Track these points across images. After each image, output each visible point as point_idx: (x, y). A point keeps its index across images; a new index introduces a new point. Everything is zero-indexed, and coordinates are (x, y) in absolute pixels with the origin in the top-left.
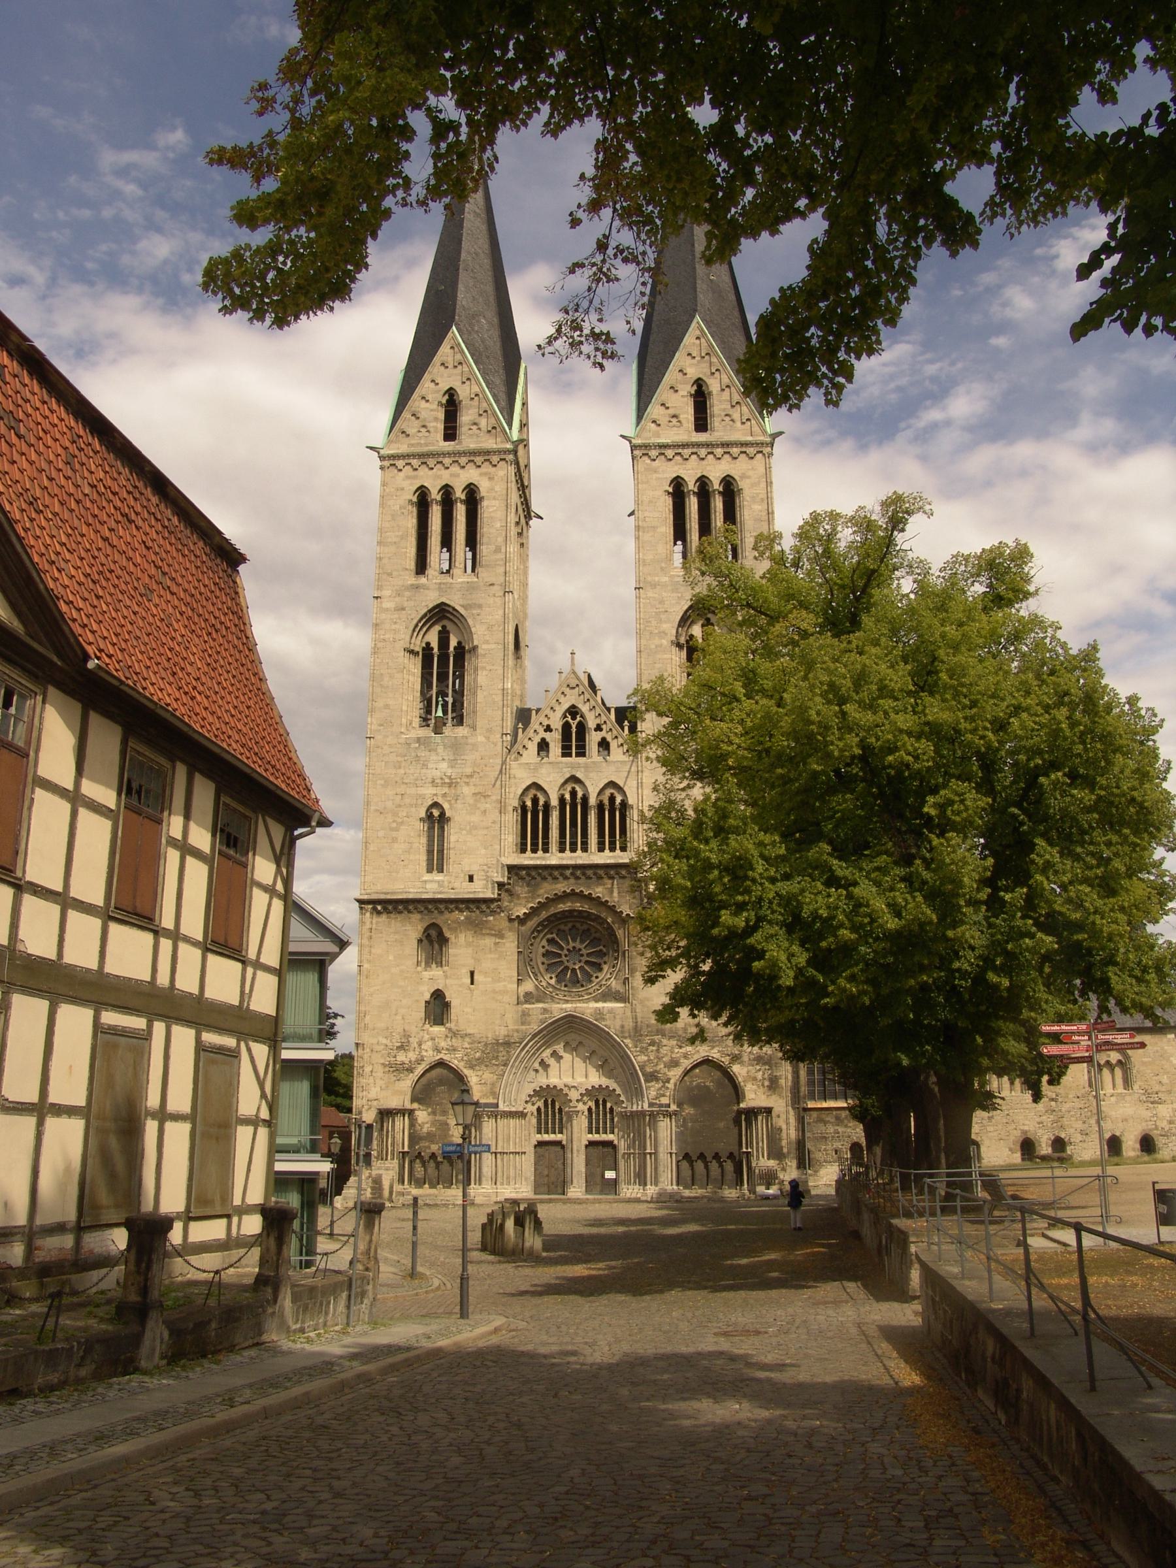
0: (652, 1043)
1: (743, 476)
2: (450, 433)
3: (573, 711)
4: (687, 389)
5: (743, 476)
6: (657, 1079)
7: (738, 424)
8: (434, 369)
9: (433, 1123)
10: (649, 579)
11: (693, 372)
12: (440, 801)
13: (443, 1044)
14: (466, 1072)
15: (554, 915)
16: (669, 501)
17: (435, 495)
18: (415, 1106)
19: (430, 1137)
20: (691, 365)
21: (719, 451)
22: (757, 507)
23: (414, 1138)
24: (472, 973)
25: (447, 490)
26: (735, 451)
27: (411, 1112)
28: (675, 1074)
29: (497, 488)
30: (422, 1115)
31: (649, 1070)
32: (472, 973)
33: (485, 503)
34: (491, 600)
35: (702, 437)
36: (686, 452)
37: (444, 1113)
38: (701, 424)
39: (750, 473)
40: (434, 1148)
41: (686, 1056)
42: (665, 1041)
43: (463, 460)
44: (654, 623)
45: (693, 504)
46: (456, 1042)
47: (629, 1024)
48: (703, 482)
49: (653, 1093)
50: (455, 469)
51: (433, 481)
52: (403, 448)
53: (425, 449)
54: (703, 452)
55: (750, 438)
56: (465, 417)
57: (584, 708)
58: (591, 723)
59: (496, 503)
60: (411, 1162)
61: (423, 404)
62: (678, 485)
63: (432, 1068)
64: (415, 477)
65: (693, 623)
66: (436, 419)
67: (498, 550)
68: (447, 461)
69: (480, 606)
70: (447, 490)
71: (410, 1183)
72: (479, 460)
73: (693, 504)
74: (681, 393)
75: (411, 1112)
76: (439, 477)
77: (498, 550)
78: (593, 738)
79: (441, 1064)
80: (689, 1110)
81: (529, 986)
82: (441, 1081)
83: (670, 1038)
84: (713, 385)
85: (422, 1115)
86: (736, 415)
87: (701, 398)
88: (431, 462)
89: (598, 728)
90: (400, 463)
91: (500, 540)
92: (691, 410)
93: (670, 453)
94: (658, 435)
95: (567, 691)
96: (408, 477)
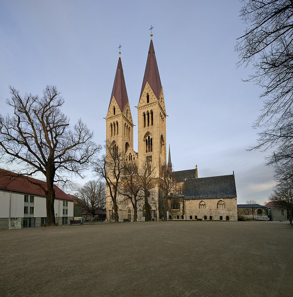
3: (130, 154)
4: (146, 95)
7: (153, 100)
11: (146, 92)
23: (113, 214)
26: (152, 105)
29: (120, 121)
36: (145, 107)
43: (116, 117)
44: (140, 138)
45: (146, 116)
48: (148, 112)
54: (148, 106)
57: (131, 153)
58: (132, 155)
62: (144, 113)
65: (147, 136)
68: (114, 118)
73: (146, 116)
74: (145, 96)
75: (112, 210)
78: (133, 157)
84: (149, 94)
87: (148, 97)
89: (133, 156)
93: (143, 108)
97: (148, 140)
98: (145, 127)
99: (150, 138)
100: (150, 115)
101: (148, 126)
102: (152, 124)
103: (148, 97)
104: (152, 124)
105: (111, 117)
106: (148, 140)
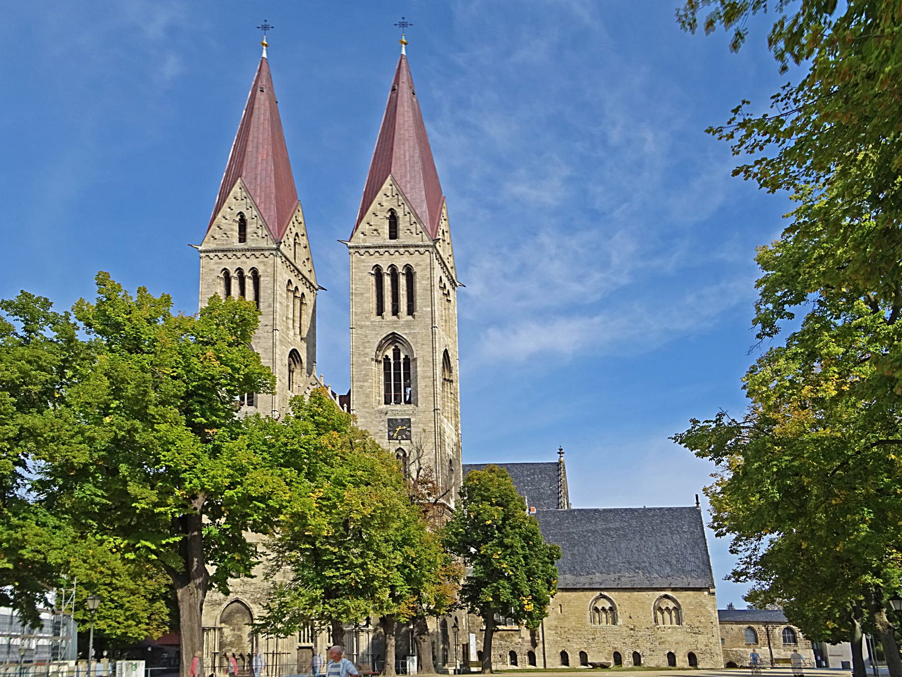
1: (417, 265)
2: (243, 238)
5: (417, 265)
8: (230, 200)
9: (233, 636)
10: (359, 323)
11: (387, 205)
13: (238, 589)
14: (251, 606)
16: (373, 279)
17: (234, 274)
18: (223, 625)
19: (232, 644)
20: (386, 201)
21: (402, 250)
22: (424, 282)
23: (222, 645)
25: (240, 271)
26: (412, 250)
27: (220, 629)
29: (269, 270)
30: (227, 631)
33: (262, 279)
34: (266, 334)
35: (393, 242)
36: (382, 251)
37: (240, 629)
38: (393, 235)
39: (421, 263)
40: (234, 650)
43: (248, 254)
45: (387, 281)
46: (247, 588)
50: (244, 259)
51: (232, 266)
52: (212, 246)
53: (225, 247)
54: (392, 251)
55: (421, 243)
56: (249, 230)
59: (268, 279)
60: (220, 658)
61: (224, 221)
62: (378, 269)
63: (232, 603)
64: (221, 263)
66: (232, 230)
67: (269, 306)
68: (239, 254)
69: (259, 338)
70: (240, 271)
71: (220, 671)
72: (257, 254)
73: (387, 281)
74: (380, 217)
76: (235, 263)
77: (269, 306)
79: (237, 601)
82: (238, 611)
84: (400, 213)
85: (227, 631)
86: (413, 230)
87: (393, 220)
88: (230, 254)
90: (212, 255)
91: (271, 300)
92: (387, 227)
93: (372, 251)
94: (365, 241)
95: (311, 387)
96: (216, 263)
97: (392, 361)
98: (380, 311)
99: (402, 356)
100: (403, 281)
101: (395, 312)
102: (411, 311)
103: (393, 220)
104: (411, 311)
105: (229, 251)
106: (392, 361)
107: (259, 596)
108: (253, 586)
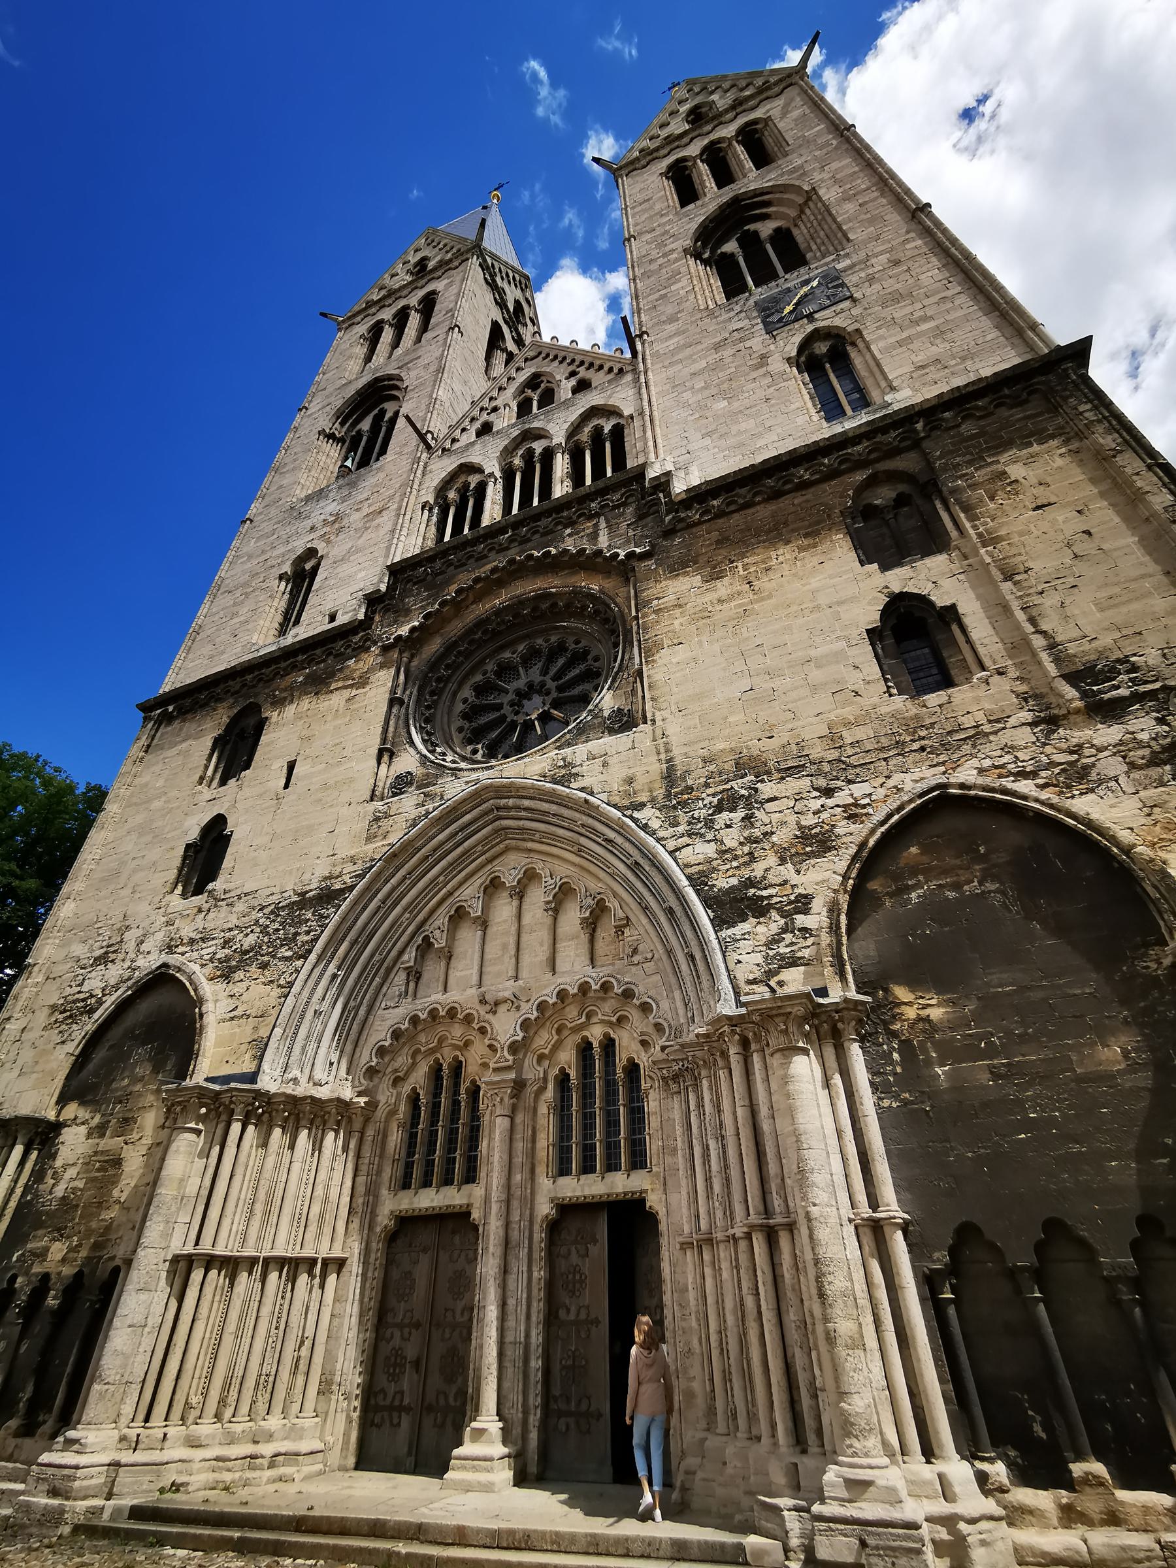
0: (729, 802)
6: (760, 909)
12: (315, 544)
15: (480, 623)
24: (291, 766)
28: (824, 878)
31: (723, 882)
32: (291, 766)
41: (853, 813)
42: (767, 789)
47: (649, 770)
49: (750, 961)
80: (920, 1006)
81: (407, 762)
83: (787, 773)
107: (251, 940)
108: (240, 907)
